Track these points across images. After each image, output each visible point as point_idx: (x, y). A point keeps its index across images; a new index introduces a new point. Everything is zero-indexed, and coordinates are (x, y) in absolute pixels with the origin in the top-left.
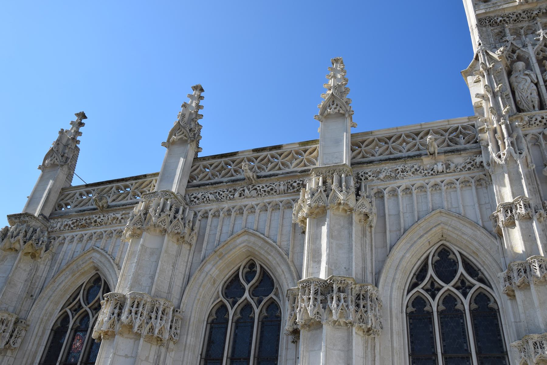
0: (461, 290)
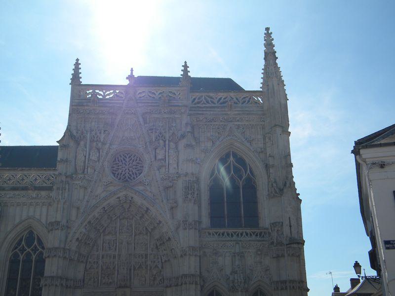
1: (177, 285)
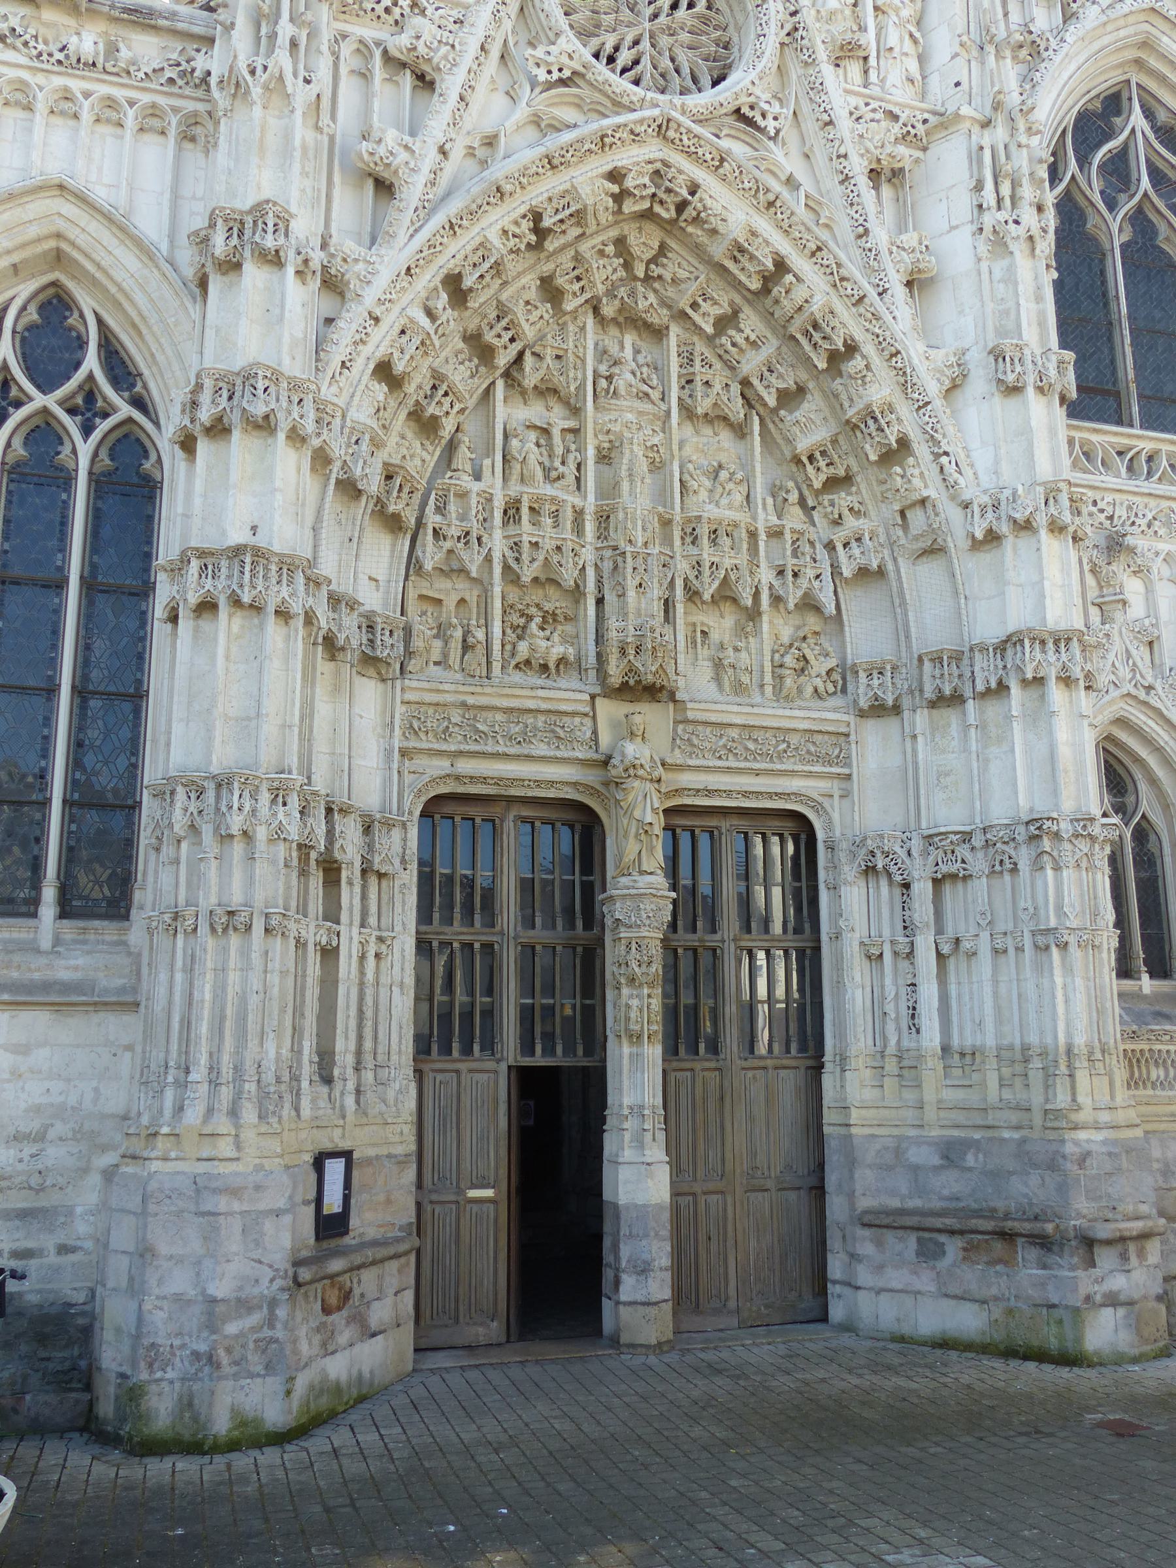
0: (79, 418)
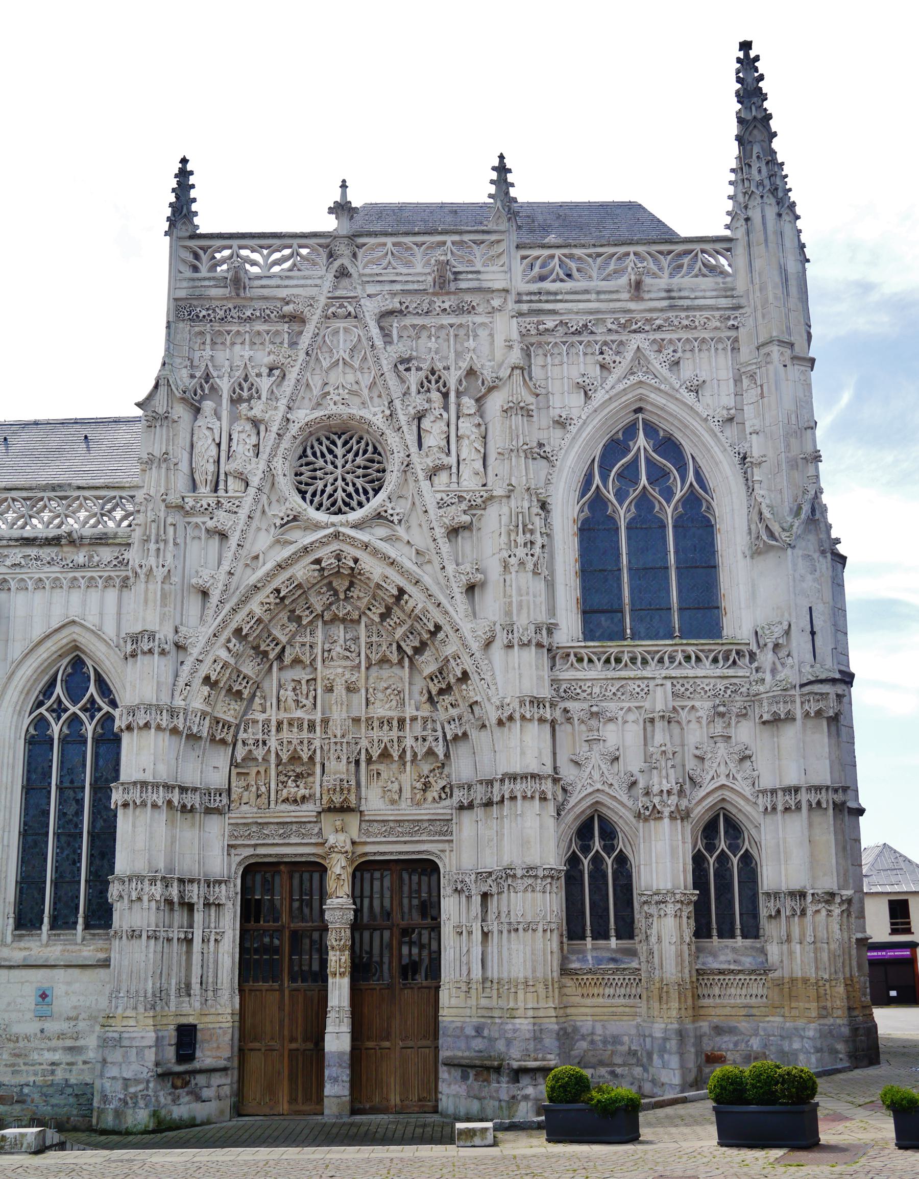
0: (88, 714)
1: (489, 804)
